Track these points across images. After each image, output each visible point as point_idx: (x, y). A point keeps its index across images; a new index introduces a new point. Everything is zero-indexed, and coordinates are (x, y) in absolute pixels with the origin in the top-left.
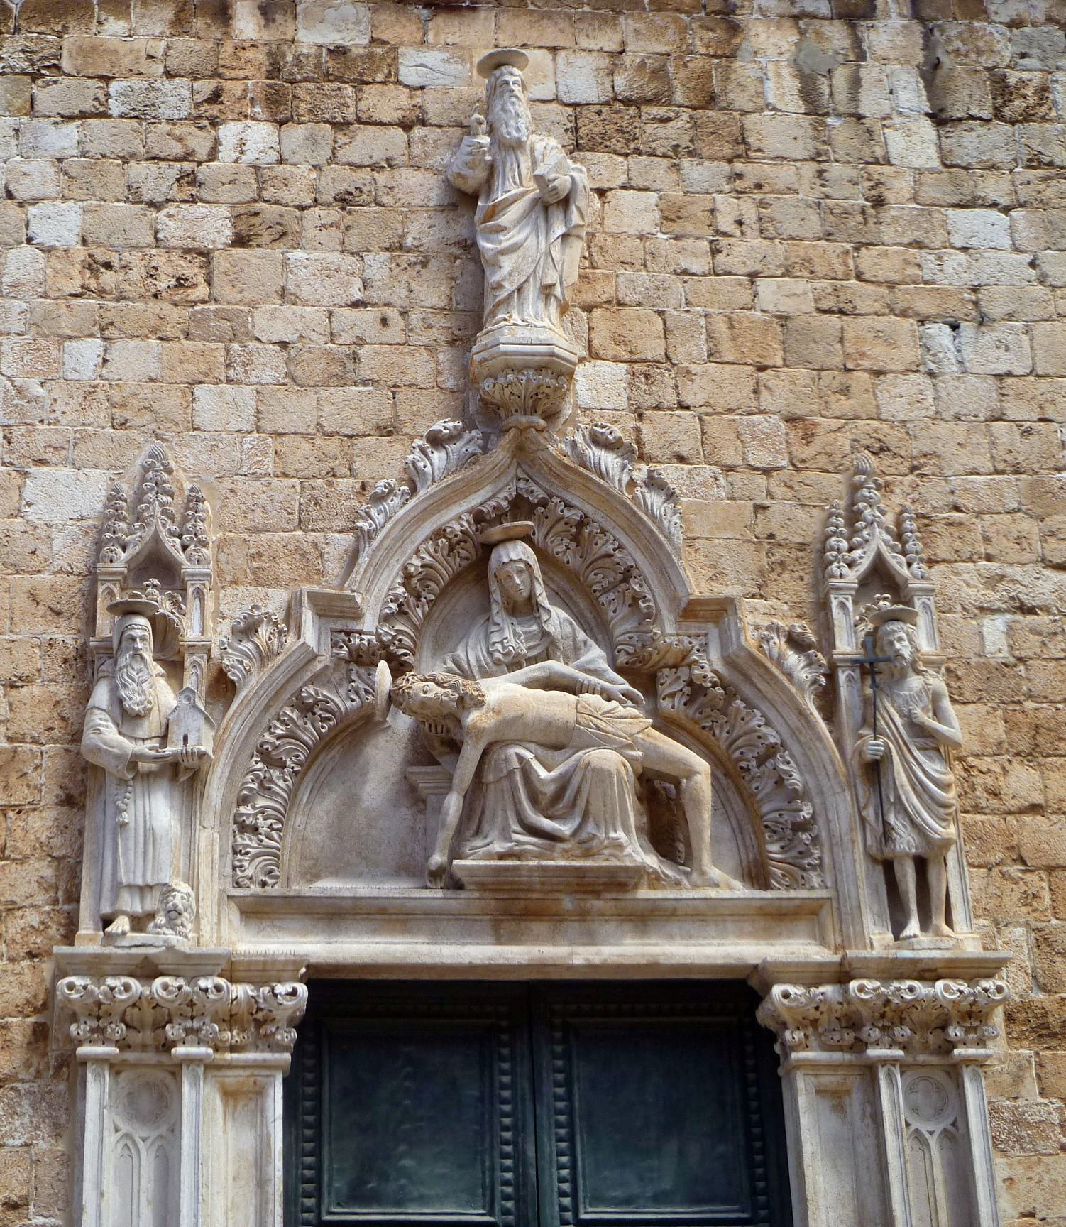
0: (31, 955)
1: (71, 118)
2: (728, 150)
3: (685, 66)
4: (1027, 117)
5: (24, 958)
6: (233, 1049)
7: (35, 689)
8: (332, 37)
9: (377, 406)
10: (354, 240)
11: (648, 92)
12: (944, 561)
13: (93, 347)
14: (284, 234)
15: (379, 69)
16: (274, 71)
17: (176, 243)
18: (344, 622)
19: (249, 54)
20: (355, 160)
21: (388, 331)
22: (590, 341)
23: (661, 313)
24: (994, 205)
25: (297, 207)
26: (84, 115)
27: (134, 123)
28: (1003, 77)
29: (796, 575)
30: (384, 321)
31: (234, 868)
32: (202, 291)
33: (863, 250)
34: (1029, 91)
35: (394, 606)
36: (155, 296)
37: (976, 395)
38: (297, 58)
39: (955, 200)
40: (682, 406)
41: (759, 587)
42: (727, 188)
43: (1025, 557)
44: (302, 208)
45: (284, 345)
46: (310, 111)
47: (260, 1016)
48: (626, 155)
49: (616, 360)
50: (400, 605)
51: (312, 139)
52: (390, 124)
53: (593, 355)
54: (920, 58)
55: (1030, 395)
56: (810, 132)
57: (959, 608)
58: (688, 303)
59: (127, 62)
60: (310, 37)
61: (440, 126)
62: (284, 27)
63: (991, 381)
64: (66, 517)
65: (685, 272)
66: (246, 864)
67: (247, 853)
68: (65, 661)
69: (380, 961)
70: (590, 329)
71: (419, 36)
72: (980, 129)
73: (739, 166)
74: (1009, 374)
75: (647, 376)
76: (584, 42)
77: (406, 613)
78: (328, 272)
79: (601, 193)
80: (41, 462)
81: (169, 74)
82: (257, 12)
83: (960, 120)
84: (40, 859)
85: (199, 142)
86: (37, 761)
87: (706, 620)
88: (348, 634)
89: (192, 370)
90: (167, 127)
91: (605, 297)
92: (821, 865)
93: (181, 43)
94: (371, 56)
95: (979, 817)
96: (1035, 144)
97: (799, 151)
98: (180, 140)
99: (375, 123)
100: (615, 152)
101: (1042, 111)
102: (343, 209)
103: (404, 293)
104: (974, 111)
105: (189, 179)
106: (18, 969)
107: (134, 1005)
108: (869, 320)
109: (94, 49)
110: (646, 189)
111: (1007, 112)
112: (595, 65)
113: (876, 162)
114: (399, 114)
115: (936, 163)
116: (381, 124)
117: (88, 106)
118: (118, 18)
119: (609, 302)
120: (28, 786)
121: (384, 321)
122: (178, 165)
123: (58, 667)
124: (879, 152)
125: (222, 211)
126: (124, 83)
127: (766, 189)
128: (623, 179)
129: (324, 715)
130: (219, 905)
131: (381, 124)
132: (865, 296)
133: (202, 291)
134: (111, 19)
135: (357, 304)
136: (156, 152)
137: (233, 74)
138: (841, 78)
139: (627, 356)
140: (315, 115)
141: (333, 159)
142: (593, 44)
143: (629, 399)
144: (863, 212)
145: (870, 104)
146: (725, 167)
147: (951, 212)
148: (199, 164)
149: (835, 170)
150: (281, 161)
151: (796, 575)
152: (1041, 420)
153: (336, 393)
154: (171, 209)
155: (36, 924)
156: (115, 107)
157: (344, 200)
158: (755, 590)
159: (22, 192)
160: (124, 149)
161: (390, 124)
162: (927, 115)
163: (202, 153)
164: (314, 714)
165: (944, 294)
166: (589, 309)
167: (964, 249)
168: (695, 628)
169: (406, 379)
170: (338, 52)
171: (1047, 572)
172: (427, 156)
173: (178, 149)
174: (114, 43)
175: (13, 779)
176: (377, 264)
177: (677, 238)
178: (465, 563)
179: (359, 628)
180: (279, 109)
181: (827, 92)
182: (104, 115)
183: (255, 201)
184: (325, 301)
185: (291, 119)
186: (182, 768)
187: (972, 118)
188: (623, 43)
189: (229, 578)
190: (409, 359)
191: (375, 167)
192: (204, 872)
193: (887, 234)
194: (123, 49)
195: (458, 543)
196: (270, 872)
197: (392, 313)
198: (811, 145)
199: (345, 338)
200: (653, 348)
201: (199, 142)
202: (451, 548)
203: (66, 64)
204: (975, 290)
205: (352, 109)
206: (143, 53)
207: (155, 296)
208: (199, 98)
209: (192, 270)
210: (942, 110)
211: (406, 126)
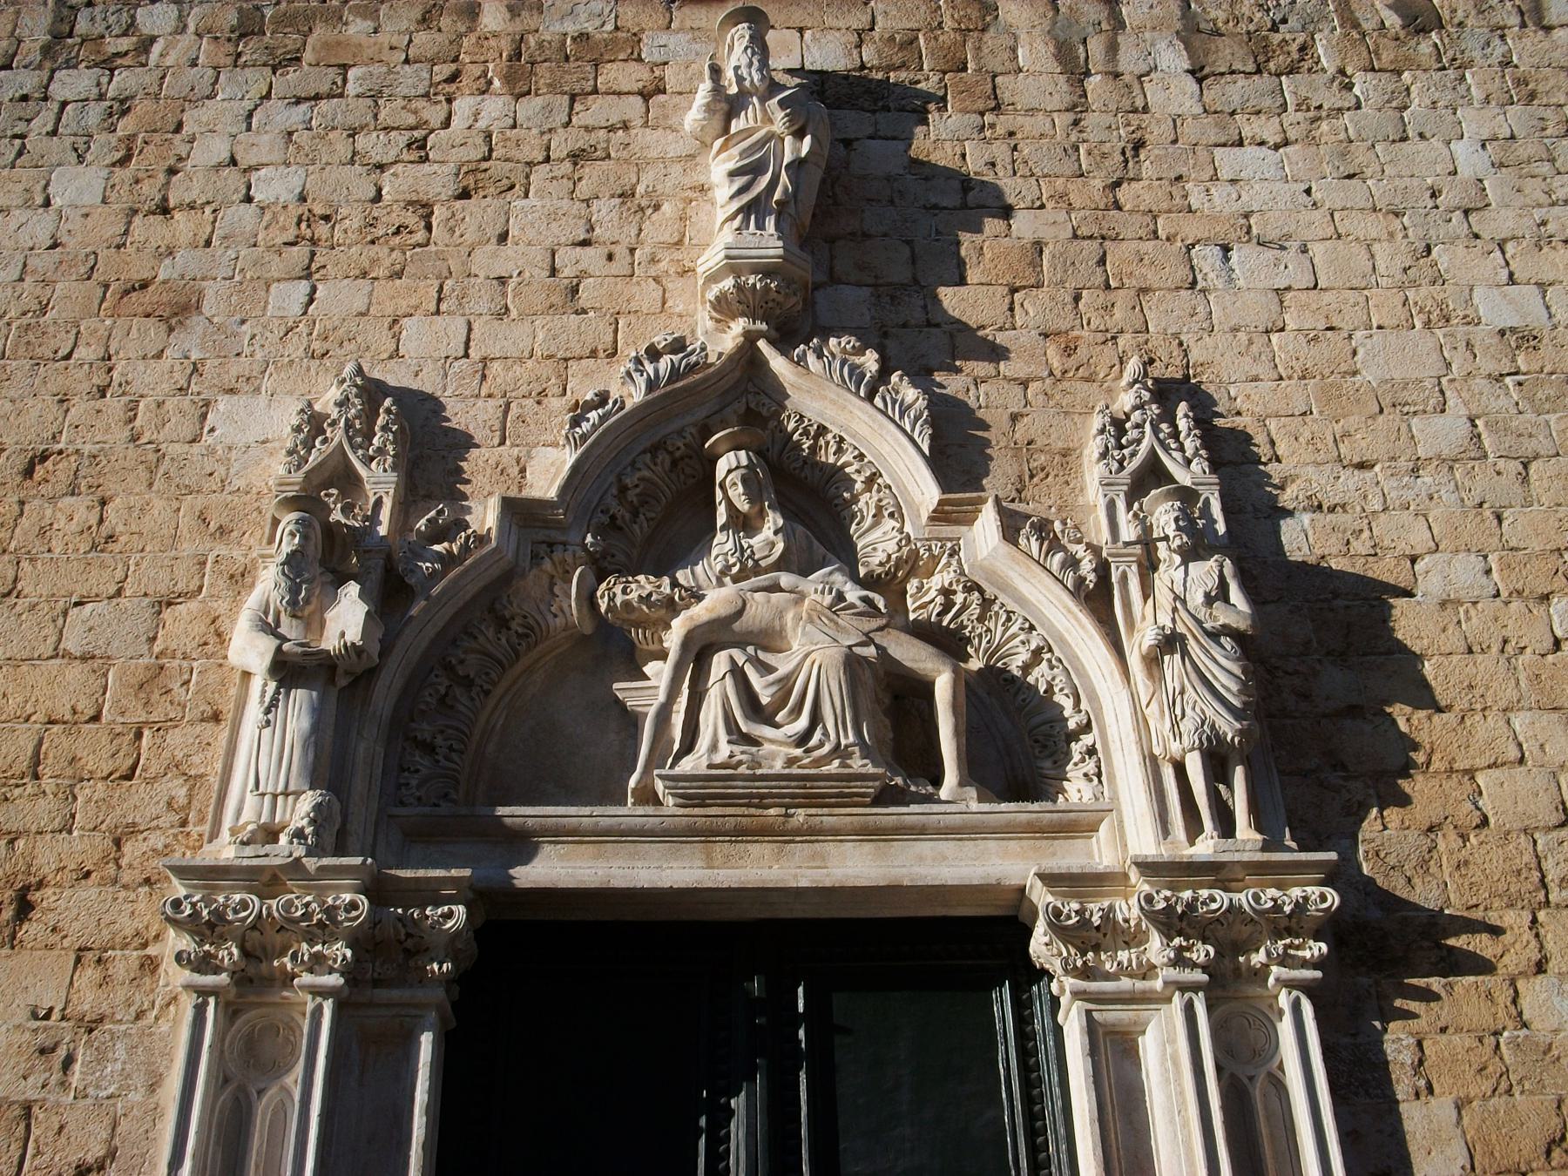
0: (147, 881)
1: (307, 99)
2: (980, 105)
3: (936, 39)
4: (1292, 70)
5: (140, 885)
6: (377, 983)
7: (193, 605)
8: (571, 28)
9: (596, 330)
10: (584, 189)
11: (897, 60)
12: (1230, 462)
13: (304, 287)
14: (512, 187)
15: (622, 49)
16: (517, 55)
17: (401, 197)
18: (547, 532)
19: (492, 42)
20: (590, 122)
21: (614, 264)
22: (831, 269)
23: (908, 242)
24: (1262, 143)
25: (527, 163)
26: (317, 97)
27: (369, 102)
28: (1266, 38)
29: (1061, 480)
30: (610, 257)
31: (399, 787)
32: (420, 236)
33: (1125, 185)
34: (1294, 47)
35: (605, 519)
36: (373, 242)
37: (1257, 310)
38: (540, 45)
39: (1223, 140)
40: (929, 324)
41: (1019, 491)
42: (975, 136)
43: (1321, 457)
44: (530, 164)
45: (502, 280)
46: (550, 85)
47: (409, 944)
48: (874, 112)
49: (859, 285)
50: (613, 518)
51: (548, 110)
52: (628, 93)
53: (834, 279)
54: (1179, 26)
55: (1314, 306)
56: (1065, 87)
57: (1250, 508)
58: (938, 232)
59: (369, 52)
60: (554, 27)
61: (680, 93)
62: (528, 20)
63: (1271, 295)
64: (251, 439)
65: (935, 207)
66: (414, 782)
67: (417, 771)
68: (232, 576)
69: (561, 885)
70: (832, 258)
71: (663, 22)
72: (1241, 81)
73: (988, 118)
74: (1288, 289)
75: (893, 298)
76: (830, 21)
77: (620, 529)
78: (553, 216)
79: (847, 143)
80: (231, 391)
81: (407, 61)
82: (504, 10)
83: (1222, 74)
84: (176, 777)
85: (434, 114)
86: (186, 677)
87: (957, 522)
88: (551, 545)
89: (403, 305)
90: (400, 102)
91: (849, 230)
92: (1099, 775)
93: (421, 38)
94: (614, 41)
95: (1289, 722)
96: (1303, 93)
97: (1055, 102)
98: (415, 112)
99: (614, 93)
100: (863, 109)
101: (1306, 65)
102: (575, 164)
103: (634, 232)
104: (1237, 66)
105: (422, 144)
106: (133, 896)
107: (253, 927)
108: (1134, 245)
109: (339, 43)
110: (894, 138)
111: (1272, 65)
112: (843, 40)
113: (1135, 111)
114: (640, 84)
115: (1198, 109)
116: (620, 94)
117: (324, 88)
118: (365, 18)
119: (853, 234)
120: (171, 703)
121: (610, 257)
122: (408, 134)
123: (222, 583)
124: (1139, 103)
125: (451, 168)
126: (364, 69)
127: (1019, 136)
128: (870, 131)
129: (520, 630)
130: (377, 824)
131: (620, 94)
132: (1129, 225)
133: (420, 236)
134: (358, 20)
135: (585, 243)
136: (390, 122)
137: (475, 58)
138: (1096, 46)
139: (871, 281)
140: (553, 88)
141: (568, 124)
142: (841, 24)
143: (873, 318)
144: (1123, 153)
145: (1129, 61)
146: (976, 118)
147: (1218, 152)
148: (432, 131)
149: (1090, 120)
150: (514, 126)
151: (1061, 480)
152: (1328, 329)
153: (558, 321)
154: (399, 168)
155: (160, 846)
156: (351, 89)
157: (576, 157)
158: (1014, 494)
159: (245, 160)
160: (353, 120)
161: (628, 93)
162: (1188, 71)
163: (435, 122)
164: (509, 629)
165: (1214, 219)
166: (831, 240)
167: (1233, 181)
168: (947, 530)
169: (634, 306)
170: (582, 37)
171: (1349, 472)
172: (666, 117)
173: (411, 120)
174: (363, 39)
175: (155, 696)
176: (605, 210)
177: (926, 179)
178: (691, 481)
179: (563, 538)
180: (519, 83)
181: (1083, 56)
182: (341, 95)
183: (485, 159)
184: (548, 243)
185: (529, 93)
186: (340, 671)
187: (1233, 72)
188: (873, 22)
189: (422, 492)
190: (636, 289)
191: (611, 129)
192: (359, 785)
193: (1147, 169)
194: (365, 44)
195: (682, 458)
196: (446, 795)
197: (621, 251)
198: (1068, 100)
199: (567, 272)
200: (899, 273)
201: (434, 114)
202: (674, 463)
203: (308, 56)
204: (1247, 216)
205: (591, 83)
206: (386, 46)
207: (373, 242)
208: (437, 79)
209: (411, 219)
210: (1202, 68)
211: (645, 95)
